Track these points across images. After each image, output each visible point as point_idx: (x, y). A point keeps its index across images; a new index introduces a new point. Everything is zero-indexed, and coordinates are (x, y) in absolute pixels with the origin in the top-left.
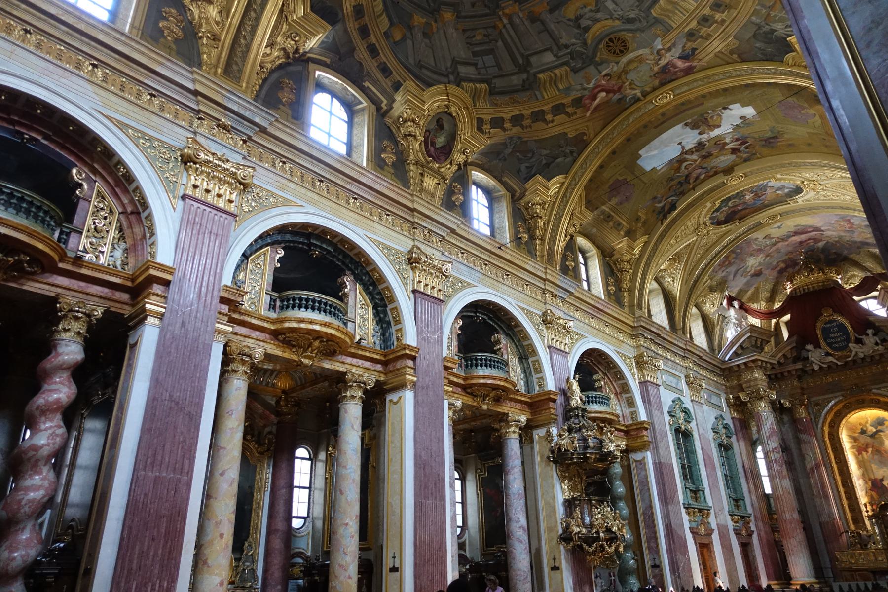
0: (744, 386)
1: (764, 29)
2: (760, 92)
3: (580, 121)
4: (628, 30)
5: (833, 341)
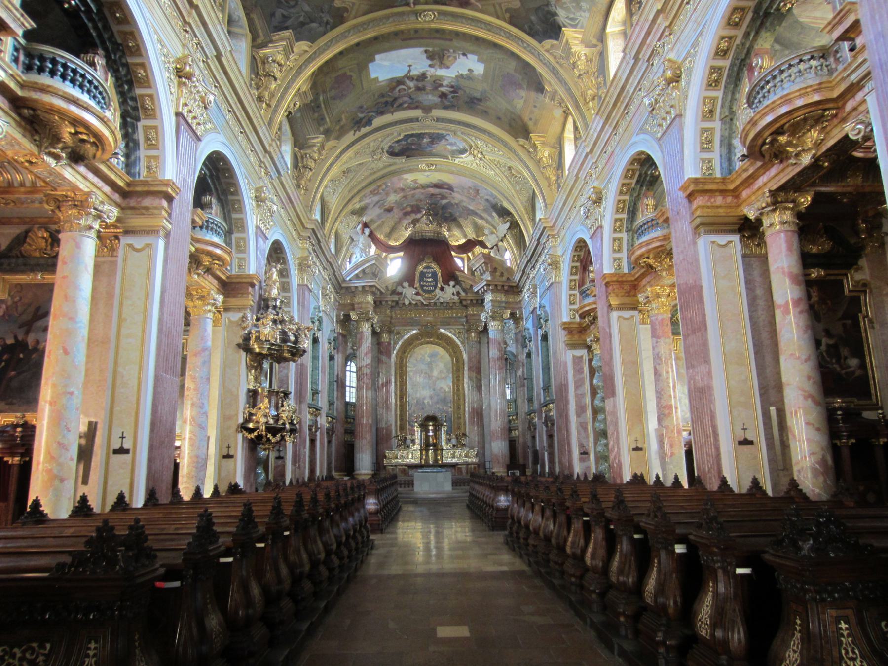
0: (356, 306)
5: (425, 284)
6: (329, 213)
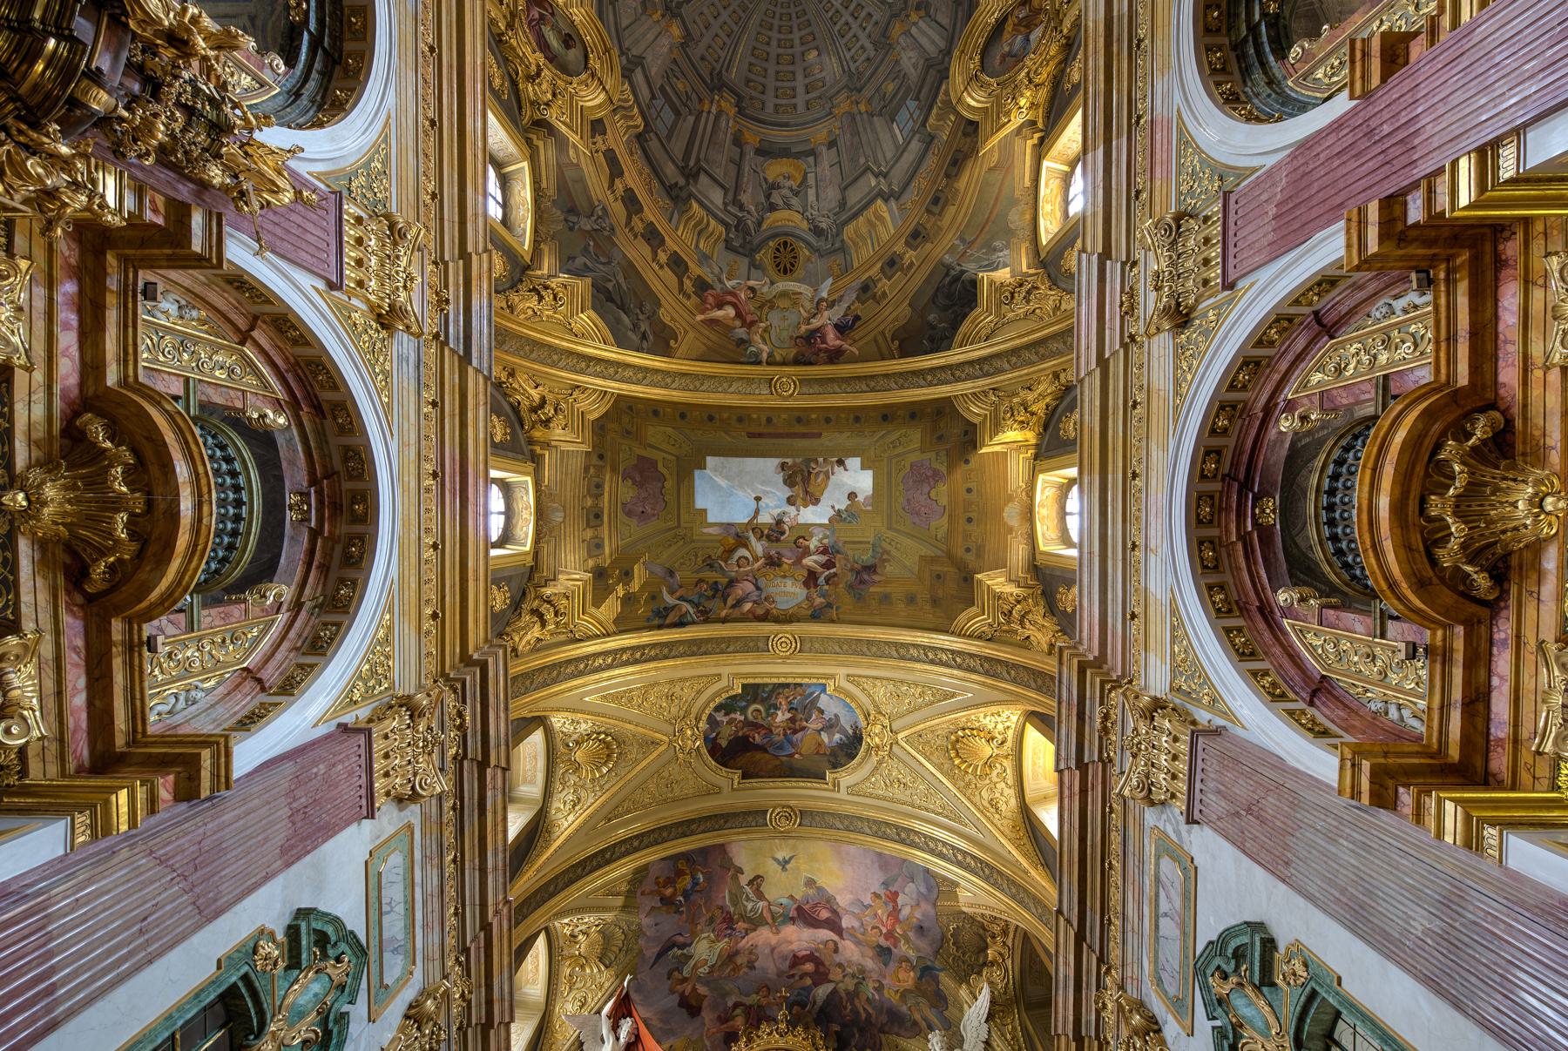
1: (953, 273)
2: (898, 434)
3: (685, 315)
4: (808, 243)
6: (547, 848)
